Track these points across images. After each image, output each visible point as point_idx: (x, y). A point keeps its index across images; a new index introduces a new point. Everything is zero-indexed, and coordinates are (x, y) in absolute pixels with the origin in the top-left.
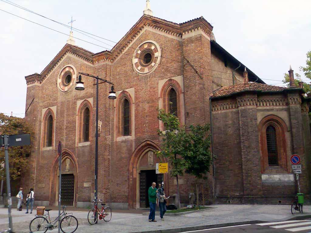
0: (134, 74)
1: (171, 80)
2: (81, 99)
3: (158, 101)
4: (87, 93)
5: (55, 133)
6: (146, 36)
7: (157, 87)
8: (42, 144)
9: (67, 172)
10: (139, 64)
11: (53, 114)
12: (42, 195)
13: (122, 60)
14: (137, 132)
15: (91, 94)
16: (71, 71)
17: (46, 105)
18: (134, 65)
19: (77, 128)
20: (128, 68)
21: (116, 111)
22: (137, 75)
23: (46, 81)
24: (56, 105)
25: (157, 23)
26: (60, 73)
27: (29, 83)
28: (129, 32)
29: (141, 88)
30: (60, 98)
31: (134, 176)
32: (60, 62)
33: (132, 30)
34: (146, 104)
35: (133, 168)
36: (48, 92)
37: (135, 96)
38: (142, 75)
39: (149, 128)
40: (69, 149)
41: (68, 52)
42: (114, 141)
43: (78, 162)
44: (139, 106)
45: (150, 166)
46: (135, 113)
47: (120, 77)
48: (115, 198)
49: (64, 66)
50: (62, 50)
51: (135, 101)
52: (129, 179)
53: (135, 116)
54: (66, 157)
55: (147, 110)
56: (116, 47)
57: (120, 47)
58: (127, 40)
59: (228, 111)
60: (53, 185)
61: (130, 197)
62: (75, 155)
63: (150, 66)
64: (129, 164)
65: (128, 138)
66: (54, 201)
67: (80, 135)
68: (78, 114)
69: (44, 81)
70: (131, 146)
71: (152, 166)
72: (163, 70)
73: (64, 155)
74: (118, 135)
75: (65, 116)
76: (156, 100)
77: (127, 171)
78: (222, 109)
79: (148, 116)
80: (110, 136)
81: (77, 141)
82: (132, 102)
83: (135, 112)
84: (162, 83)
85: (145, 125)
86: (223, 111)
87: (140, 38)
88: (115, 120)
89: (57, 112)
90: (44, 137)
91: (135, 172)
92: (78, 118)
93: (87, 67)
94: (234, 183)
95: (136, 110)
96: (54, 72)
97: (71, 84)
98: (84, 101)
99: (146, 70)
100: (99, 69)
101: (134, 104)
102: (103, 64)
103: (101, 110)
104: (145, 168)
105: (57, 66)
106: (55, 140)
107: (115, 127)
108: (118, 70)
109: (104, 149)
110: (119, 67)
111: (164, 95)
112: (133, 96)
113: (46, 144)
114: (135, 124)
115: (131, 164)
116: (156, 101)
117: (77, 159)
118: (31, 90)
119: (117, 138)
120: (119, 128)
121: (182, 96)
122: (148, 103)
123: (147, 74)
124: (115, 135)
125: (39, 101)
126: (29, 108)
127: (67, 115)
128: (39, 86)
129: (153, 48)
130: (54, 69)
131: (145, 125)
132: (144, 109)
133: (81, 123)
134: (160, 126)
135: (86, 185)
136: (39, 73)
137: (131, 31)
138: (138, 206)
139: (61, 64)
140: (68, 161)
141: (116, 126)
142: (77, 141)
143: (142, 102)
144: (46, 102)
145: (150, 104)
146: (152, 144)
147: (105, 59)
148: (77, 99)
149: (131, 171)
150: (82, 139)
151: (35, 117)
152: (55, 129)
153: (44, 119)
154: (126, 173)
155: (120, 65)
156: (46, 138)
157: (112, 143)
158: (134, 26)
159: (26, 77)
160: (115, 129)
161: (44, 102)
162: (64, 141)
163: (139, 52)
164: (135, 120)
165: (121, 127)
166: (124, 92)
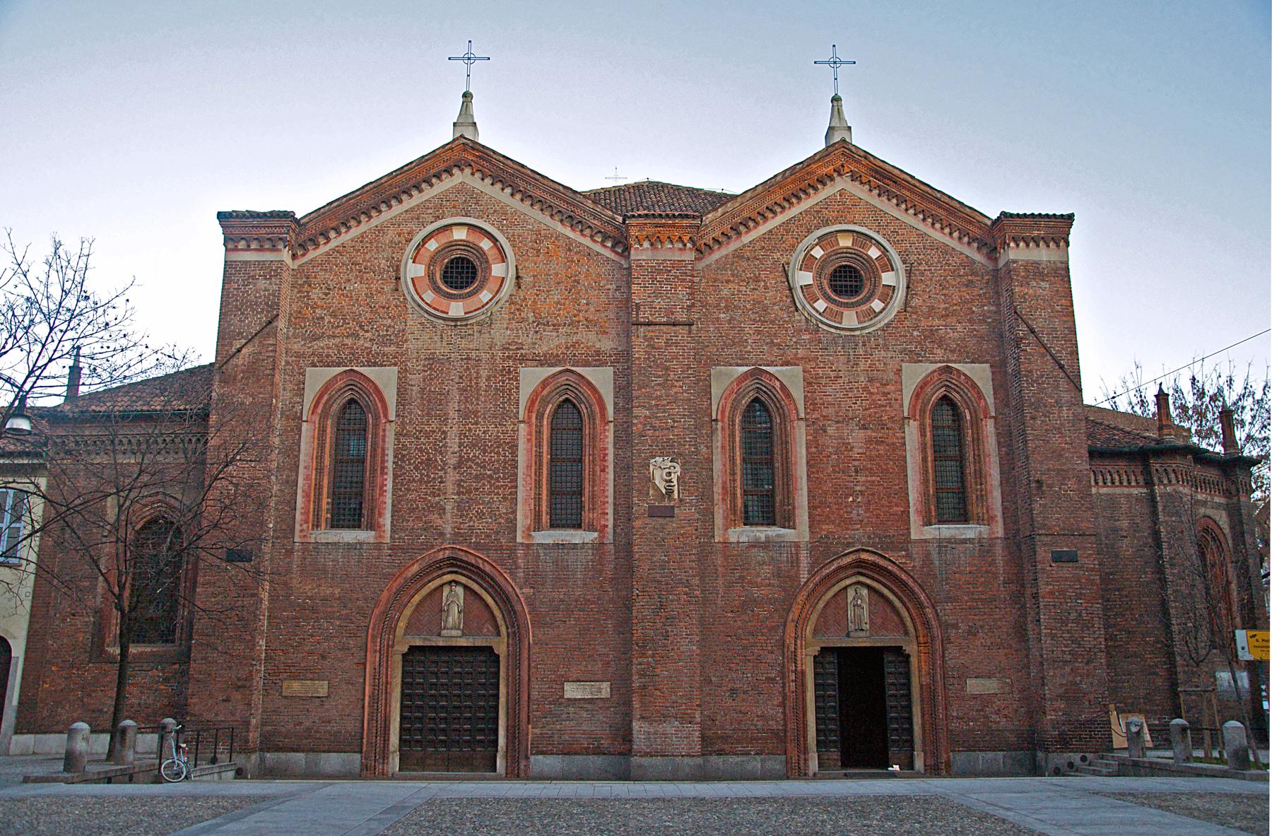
0: (800, 321)
1: (948, 369)
2: (543, 361)
3: (902, 428)
4: (573, 346)
6: (844, 207)
8: (306, 513)
11: (382, 400)
12: (309, 729)
13: (745, 264)
15: (598, 353)
16: (486, 245)
17: (328, 356)
21: (719, 432)
23: (327, 254)
24: (395, 365)
25: (885, 179)
26: (417, 239)
27: (242, 244)
30: (418, 341)
32: (417, 199)
34: (852, 431)
36: (335, 300)
38: (833, 330)
40: (477, 546)
41: (462, 170)
43: (530, 605)
45: (861, 634)
48: (725, 738)
49: (437, 218)
51: (807, 414)
52: (783, 675)
59: (1118, 491)
60: (381, 690)
62: (511, 574)
63: (864, 308)
65: (778, 536)
66: (385, 755)
68: (530, 418)
69: (312, 254)
70: (795, 562)
72: (915, 333)
73: (440, 568)
76: (893, 422)
78: (1101, 483)
81: (523, 518)
82: (794, 416)
84: (914, 374)
86: (1104, 490)
87: (818, 208)
88: (717, 466)
90: (319, 487)
92: (530, 434)
93: (569, 250)
94: (1142, 692)
96: (380, 230)
97: (485, 296)
98: (561, 372)
99: (850, 319)
101: (802, 424)
102: (677, 256)
105: (397, 209)
107: (718, 489)
110: (728, 281)
112: (798, 394)
113: (325, 515)
114: (809, 491)
116: (896, 426)
118: (253, 277)
121: (989, 428)
122: (864, 427)
124: (719, 520)
126: (244, 350)
127: (464, 415)
129: (874, 253)
130: (377, 220)
133: (539, 455)
135: (572, 691)
138: (813, 765)
139: (423, 206)
140: (454, 599)
141: (723, 488)
142: (523, 518)
145: (869, 432)
146: (882, 562)
148: (523, 360)
150: (545, 518)
152: (390, 458)
153: (319, 411)
155: (733, 275)
156: (325, 490)
159: (221, 216)
161: (315, 338)
162: (448, 515)
166: (757, 373)
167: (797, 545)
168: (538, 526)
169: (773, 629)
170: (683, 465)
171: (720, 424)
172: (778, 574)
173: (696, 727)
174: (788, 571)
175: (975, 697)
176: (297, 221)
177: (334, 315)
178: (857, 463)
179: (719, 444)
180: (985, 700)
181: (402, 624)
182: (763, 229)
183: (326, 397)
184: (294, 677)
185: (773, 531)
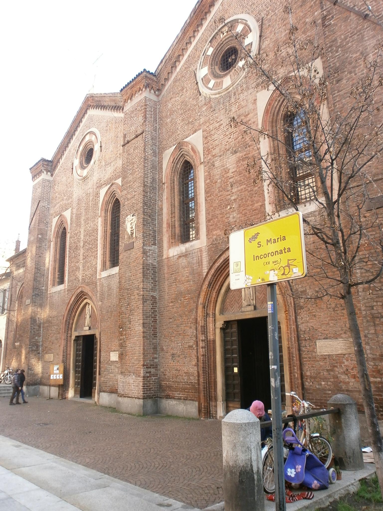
0: (201, 101)
5: (67, 258)
7: (255, 109)
9: (86, 331)
10: (210, 77)
14: (211, 227)
18: (200, 84)
19: (99, 242)
20: (189, 94)
22: (208, 101)
27: (35, 178)
28: (188, 22)
29: (217, 125)
31: (211, 337)
33: (194, 14)
35: (207, 315)
37: (204, 148)
38: (217, 96)
39: (240, 213)
42: (165, 257)
44: (214, 166)
46: (206, 184)
47: (172, 119)
48: (170, 387)
50: (81, 109)
53: (205, 191)
54: (85, 301)
55: (234, 170)
56: (164, 61)
57: (171, 60)
58: (186, 40)
61: (201, 387)
64: (197, 308)
65: (191, 246)
67: (104, 254)
69: (57, 171)
70: (200, 263)
71: (252, 308)
74: (171, 245)
75: (83, 222)
77: (192, 325)
79: (237, 182)
80: (156, 247)
82: (197, 163)
83: (205, 181)
85: (229, 208)
89: (71, 219)
90: (55, 268)
91: (211, 326)
95: (209, 176)
96: (70, 151)
98: (111, 186)
99: (227, 81)
100: (133, 112)
103: (135, 192)
104: (234, 315)
106: (68, 271)
107: (165, 225)
108: (170, 105)
109: (141, 275)
110: (171, 99)
111: (274, 122)
112: (200, 148)
114: (207, 210)
115: (200, 307)
117: (100, 303)
119: (170, 250)
120: (173, 227)
122: (236, 152)
123: (228, 91)
125: (49, 206)
126: (34, 219)
128: (49, 181)
131: (231, 208)
132: (226, 171)
133: (105, 232)
134: (267, 203)
136: (50, 159)
137: (193, 16)
140: (88, 310)
143: (220, 156)
144: (58, 206)
145: (238, 154)
147: (144, 89)
148: (100, 186)
149: (201, 322)
150: (108, 263)
151: (42, 234)
153: (55, 236)
154: (191, 328)
157: (159, 262)
158: (196, 4)
160: (165, 230)
162: (81, 272)
163: (210, 51)
164: (206, 200)
165: (177, 224)
166: (180, 146)
167: (200, 250)
168: (104, 268)
169: (190, 311)
170: (138, 216)
171: (166, 185)
172: (192, 273)
173: (141, 379)
174: (197, 269)
175: (324, 358)
176: (50, 161)
177: (59, 194)
178: (231, 180)
179: (165, 197)
180: (334, 361)
181: (74, 326)
182: (186, 57)
183: (57, 229)
184: (46, 353)
185: (188, 245)
